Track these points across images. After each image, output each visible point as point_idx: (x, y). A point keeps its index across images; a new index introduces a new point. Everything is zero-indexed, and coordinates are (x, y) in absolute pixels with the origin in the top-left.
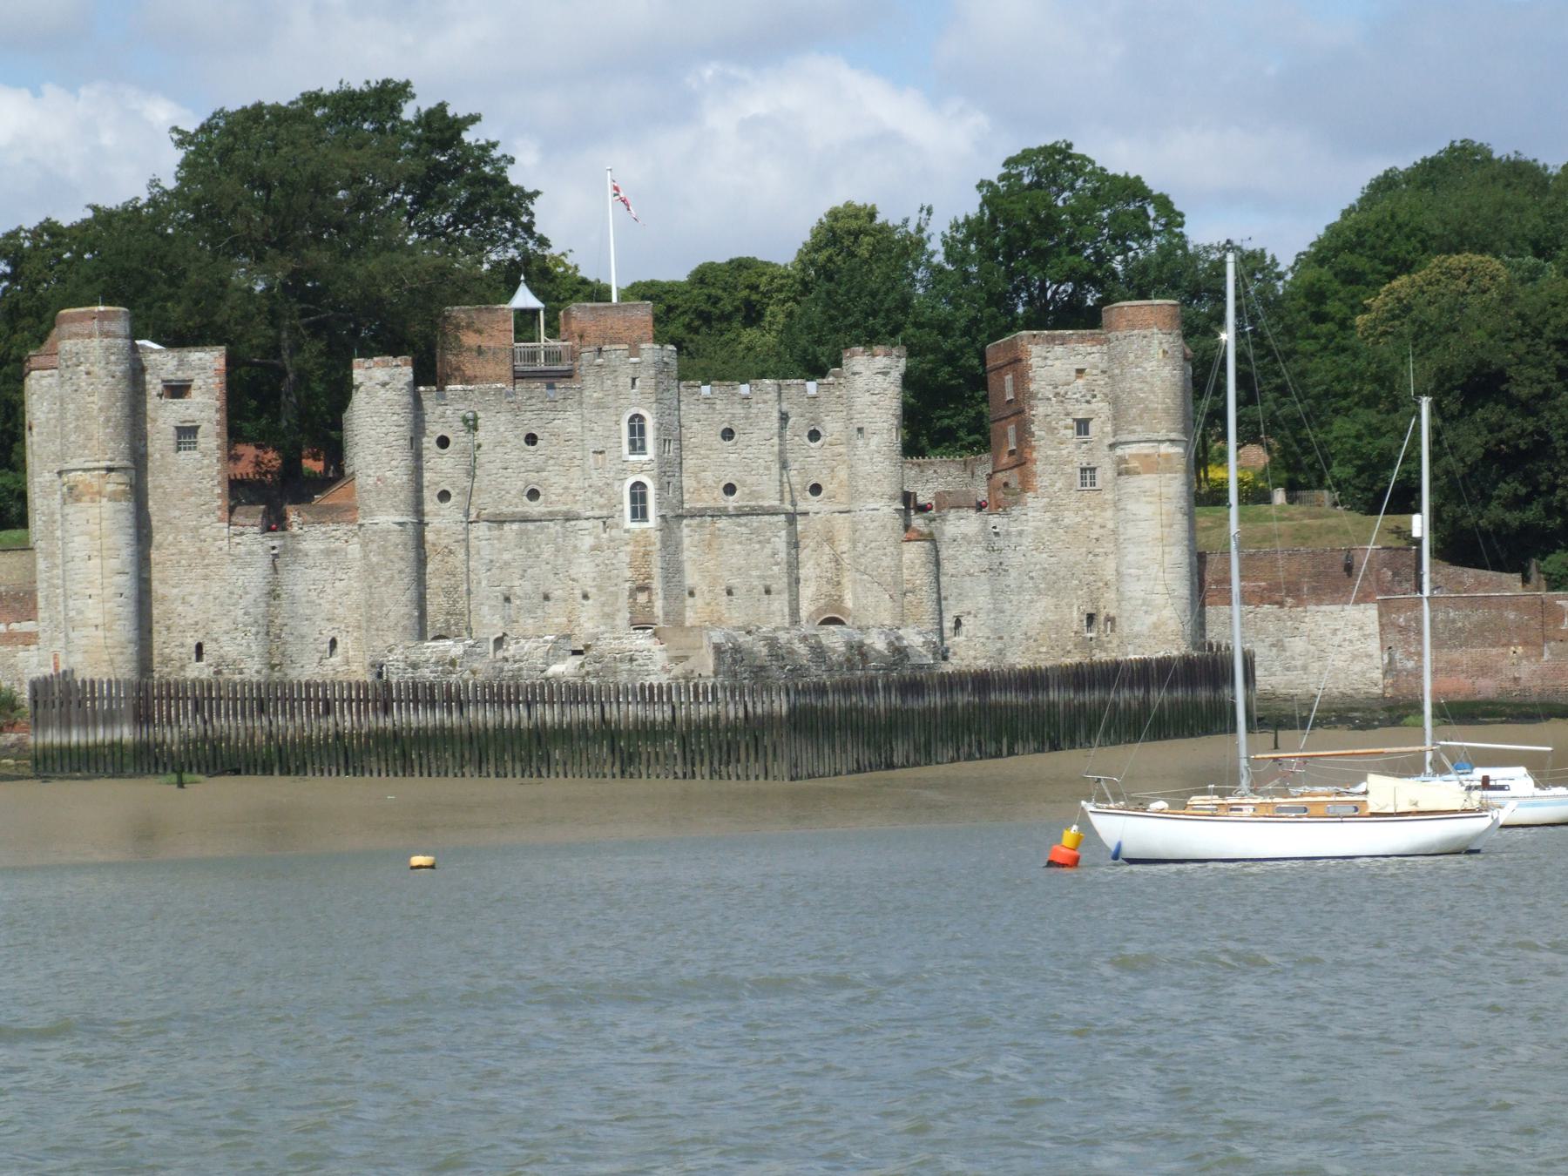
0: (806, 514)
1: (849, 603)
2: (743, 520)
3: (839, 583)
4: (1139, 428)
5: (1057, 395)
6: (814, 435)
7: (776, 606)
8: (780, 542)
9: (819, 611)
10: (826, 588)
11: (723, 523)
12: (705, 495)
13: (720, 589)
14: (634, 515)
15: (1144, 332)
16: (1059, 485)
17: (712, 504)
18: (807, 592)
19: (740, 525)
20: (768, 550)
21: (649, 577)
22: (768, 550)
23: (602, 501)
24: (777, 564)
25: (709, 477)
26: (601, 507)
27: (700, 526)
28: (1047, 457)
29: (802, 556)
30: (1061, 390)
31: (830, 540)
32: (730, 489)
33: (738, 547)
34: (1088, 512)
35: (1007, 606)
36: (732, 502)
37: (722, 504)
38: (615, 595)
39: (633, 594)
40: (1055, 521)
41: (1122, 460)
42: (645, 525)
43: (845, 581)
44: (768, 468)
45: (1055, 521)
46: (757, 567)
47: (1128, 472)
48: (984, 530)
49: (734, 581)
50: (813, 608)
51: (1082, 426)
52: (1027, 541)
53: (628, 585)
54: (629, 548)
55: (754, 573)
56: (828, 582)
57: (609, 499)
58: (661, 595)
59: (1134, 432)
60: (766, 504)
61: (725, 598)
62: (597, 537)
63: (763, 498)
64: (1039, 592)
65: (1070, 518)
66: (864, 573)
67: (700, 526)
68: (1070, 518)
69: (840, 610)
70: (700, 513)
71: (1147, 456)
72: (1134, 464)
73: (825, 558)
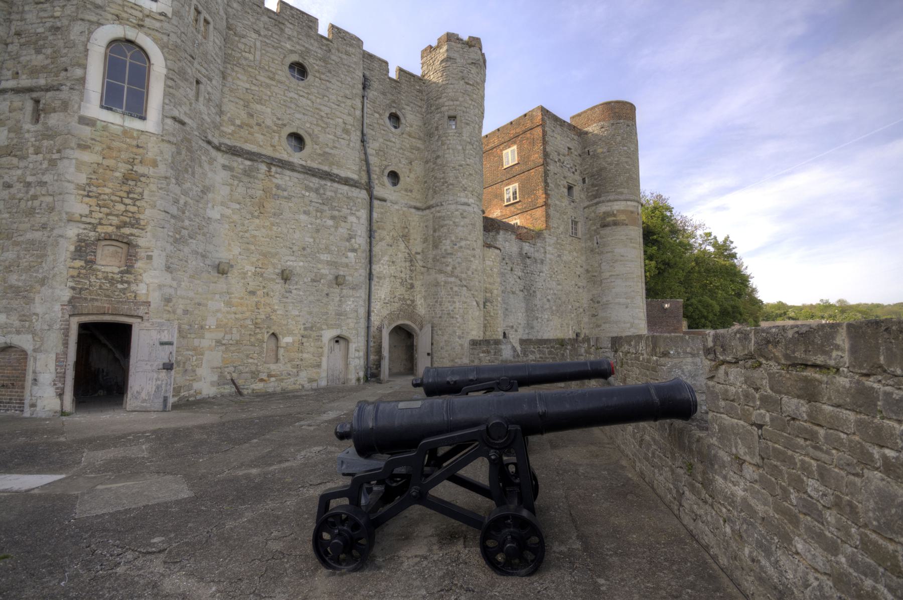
0: (383, 200)
1: (421, 309)
2: (315, 182)
3: (412, 286)
4: (626, 191)
5: (559, 160)
6: (395, 118)
7: (349, 305)
8: (358, 222)
9: (392, 316)
10: (401, 291)
11: (287, 179)
12: (259, 137)
13: (271, 272)
14: (110, 100)
15: (626, 122)
16: (561, 229)
17: (268, 151)
18: (382, 292)
19: (308, 188)
20: (343, 231)
21: (135, 223)
22: (343, 231)
23: (39, 60)
24: (354, 250)
25: (267, 113)
26: (34, 72)
27: (247, 173)
28: (556, 205)
29: (376, 249)
30: (562, 158)
31: (406, 237)
32: (297, 139)
33: (303, 217)
34: (575, 254)
35: (535, 322)
36: (297, 158)
37: (285, 156)
38: (39, 250)
39: (84, 250)
40: (559, 256)
41: (607, 214)
42: (135, 124)
43: (417, 284)
44: (346, 131)
45: (559, 256)
46: (327, 249)
47: (615, 224)
48: (520, 254)
49: (297, 264)
50: (385, 312)
51: (570, 188)
52: (545, 268)
53: (72, 232)
54: (87, 157)
55: (325, 257)
56: (402, 284)
57: (54, 58)
58: (159, 260)
59: (622, 193)
60: (343, 174)
61: (278, 287)
62: (16, 130)
63: (339, 165)
64: (552, 313)
65: (567, 257)
66: (452, 275)
67: (247, 173)
68: (567, 257)
69: (412, 316)
70: (252, 156)
71: (632, 212)
72: (622, 217)
73: (400, 255)
